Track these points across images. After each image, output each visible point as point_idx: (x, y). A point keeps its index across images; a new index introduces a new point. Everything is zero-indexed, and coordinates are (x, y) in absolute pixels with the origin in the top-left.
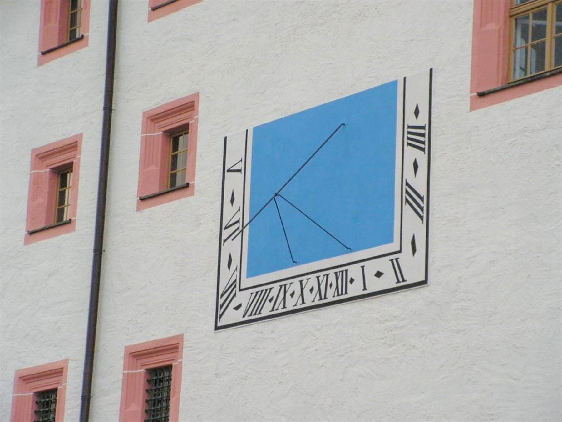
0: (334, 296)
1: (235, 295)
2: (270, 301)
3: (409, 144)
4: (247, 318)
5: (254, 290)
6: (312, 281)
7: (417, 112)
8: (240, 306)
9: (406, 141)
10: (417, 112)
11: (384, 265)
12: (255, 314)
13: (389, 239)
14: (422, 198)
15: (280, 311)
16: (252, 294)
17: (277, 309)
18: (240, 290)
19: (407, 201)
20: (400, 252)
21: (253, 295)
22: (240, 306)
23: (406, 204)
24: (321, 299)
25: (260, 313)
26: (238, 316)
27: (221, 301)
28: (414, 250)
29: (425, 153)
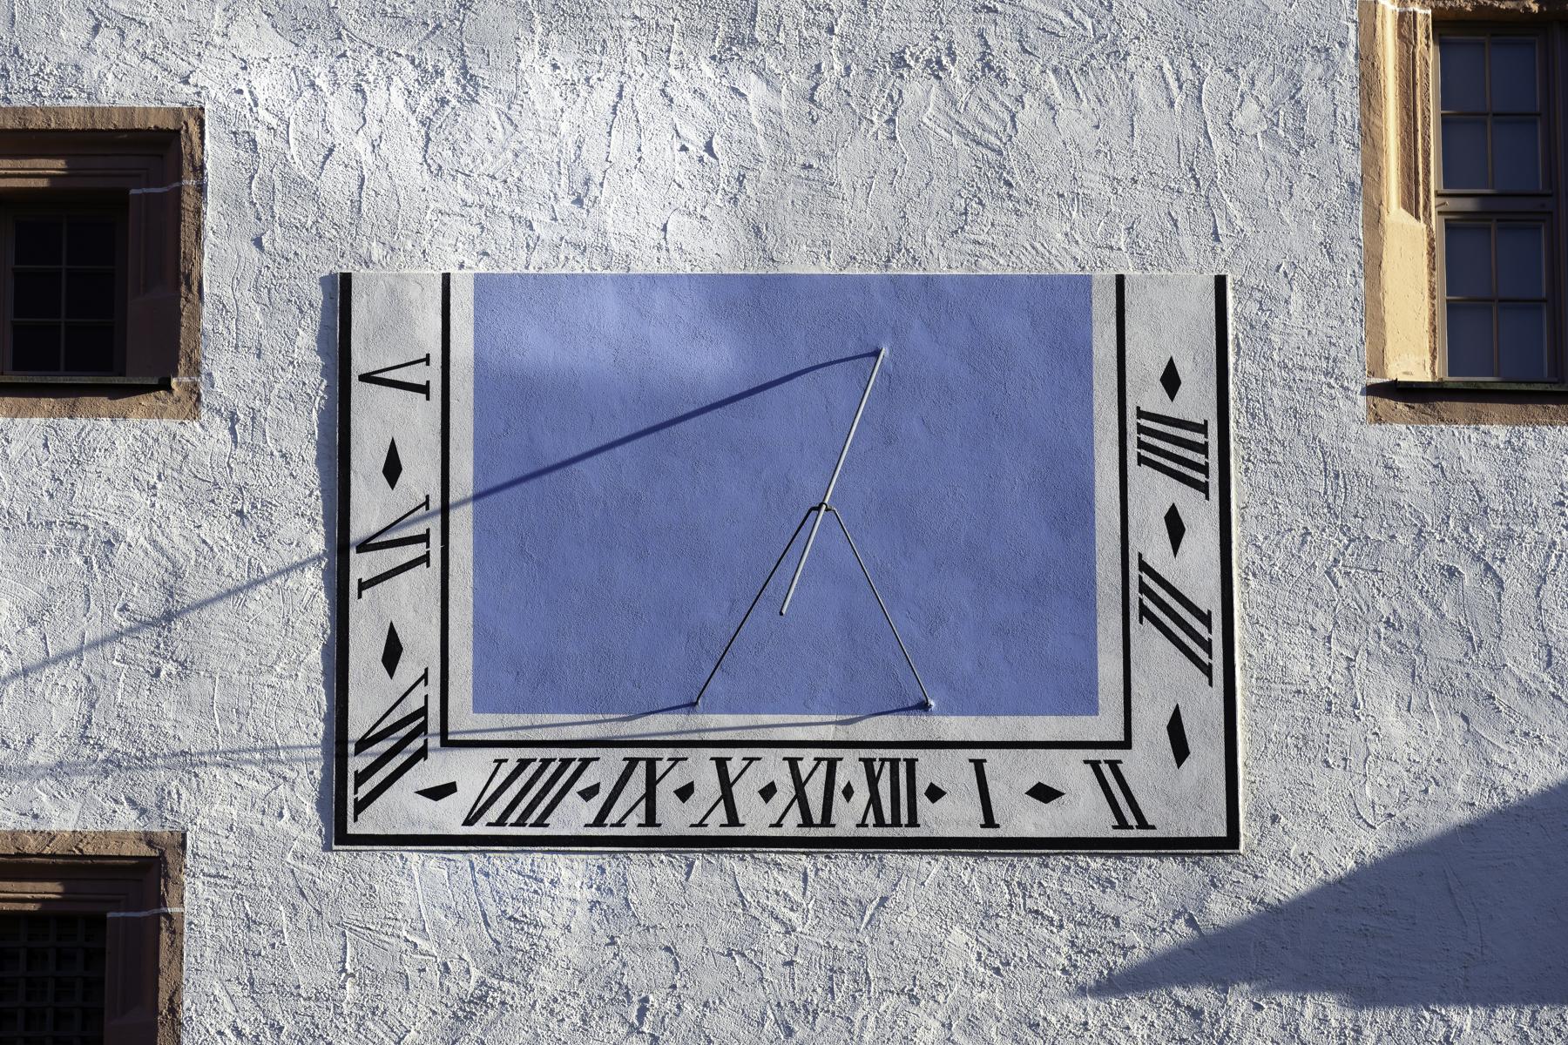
0: (863, 824)
1: (422, 753)
2: (588, 794)
3: (1142, 460)
4: (479, 829)
5: (513, 755)
6: (773, 766)
7: (1171, 381)
8: (448, 789)
9: (1133, 451)
10: (1171, 381)
11: (1070, 771)
12: (520, 823)
13: (1087, 703)
14: (1206, 619)
15: (632, 829)
16: (500, 762)
17: (620, 824)
18: (446, 743)
19: (1144, 611)
20: (1126, 744)
21: (505, 771)
22: (448, 789)
23: (1141, 622)
24: (807, 821)
25: (540, 823)
26: (448, 817)
27: (357, 764)
28: (1181, 750)
29: (1207, 498)
